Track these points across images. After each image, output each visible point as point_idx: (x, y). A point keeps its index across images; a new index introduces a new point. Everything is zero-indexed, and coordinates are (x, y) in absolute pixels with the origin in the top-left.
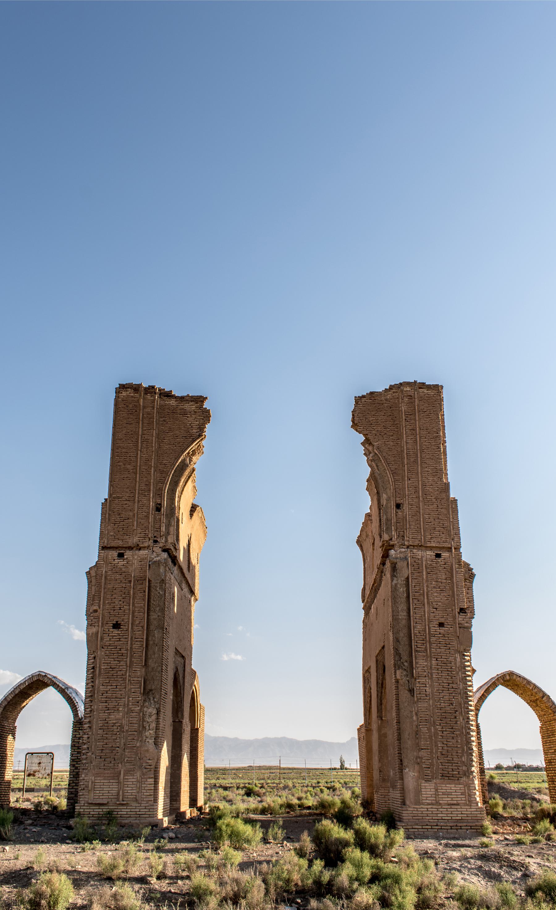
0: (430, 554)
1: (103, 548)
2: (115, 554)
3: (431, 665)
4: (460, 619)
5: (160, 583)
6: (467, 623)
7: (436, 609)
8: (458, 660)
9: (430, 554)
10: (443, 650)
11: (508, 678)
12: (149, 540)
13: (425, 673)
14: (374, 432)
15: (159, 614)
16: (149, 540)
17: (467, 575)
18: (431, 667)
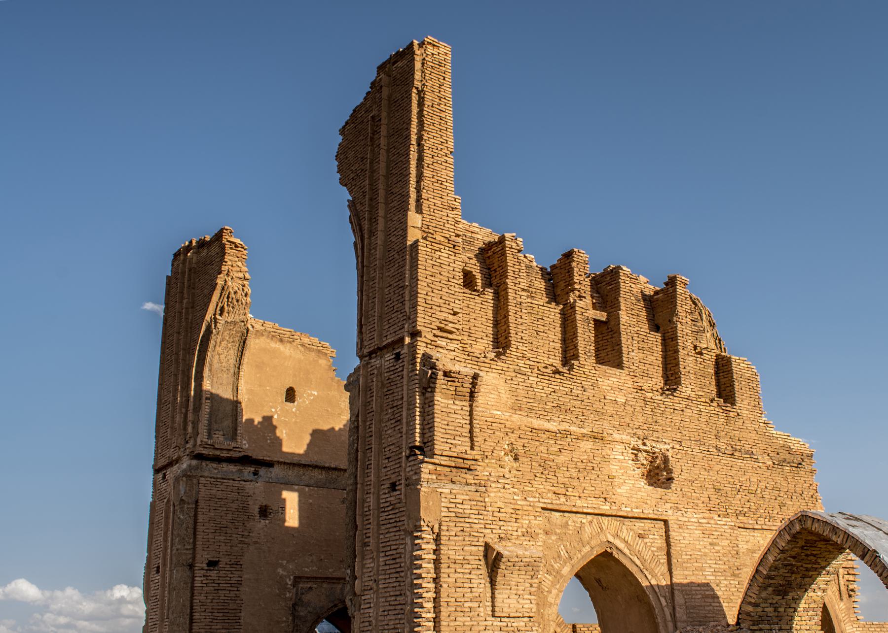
0: (389, 356)
1: (157, 471)
2: (160, 475)
3: (379, 566)
4: (408, 469)
6: (416, 473)
7: (388, 458)
8: (408, 548)
9: (389, 356)
10: (392, 534)
11: (798, 527)
13: (371, 583)
14: (352, 176)
17: (424, 380)
18: (378, 570)
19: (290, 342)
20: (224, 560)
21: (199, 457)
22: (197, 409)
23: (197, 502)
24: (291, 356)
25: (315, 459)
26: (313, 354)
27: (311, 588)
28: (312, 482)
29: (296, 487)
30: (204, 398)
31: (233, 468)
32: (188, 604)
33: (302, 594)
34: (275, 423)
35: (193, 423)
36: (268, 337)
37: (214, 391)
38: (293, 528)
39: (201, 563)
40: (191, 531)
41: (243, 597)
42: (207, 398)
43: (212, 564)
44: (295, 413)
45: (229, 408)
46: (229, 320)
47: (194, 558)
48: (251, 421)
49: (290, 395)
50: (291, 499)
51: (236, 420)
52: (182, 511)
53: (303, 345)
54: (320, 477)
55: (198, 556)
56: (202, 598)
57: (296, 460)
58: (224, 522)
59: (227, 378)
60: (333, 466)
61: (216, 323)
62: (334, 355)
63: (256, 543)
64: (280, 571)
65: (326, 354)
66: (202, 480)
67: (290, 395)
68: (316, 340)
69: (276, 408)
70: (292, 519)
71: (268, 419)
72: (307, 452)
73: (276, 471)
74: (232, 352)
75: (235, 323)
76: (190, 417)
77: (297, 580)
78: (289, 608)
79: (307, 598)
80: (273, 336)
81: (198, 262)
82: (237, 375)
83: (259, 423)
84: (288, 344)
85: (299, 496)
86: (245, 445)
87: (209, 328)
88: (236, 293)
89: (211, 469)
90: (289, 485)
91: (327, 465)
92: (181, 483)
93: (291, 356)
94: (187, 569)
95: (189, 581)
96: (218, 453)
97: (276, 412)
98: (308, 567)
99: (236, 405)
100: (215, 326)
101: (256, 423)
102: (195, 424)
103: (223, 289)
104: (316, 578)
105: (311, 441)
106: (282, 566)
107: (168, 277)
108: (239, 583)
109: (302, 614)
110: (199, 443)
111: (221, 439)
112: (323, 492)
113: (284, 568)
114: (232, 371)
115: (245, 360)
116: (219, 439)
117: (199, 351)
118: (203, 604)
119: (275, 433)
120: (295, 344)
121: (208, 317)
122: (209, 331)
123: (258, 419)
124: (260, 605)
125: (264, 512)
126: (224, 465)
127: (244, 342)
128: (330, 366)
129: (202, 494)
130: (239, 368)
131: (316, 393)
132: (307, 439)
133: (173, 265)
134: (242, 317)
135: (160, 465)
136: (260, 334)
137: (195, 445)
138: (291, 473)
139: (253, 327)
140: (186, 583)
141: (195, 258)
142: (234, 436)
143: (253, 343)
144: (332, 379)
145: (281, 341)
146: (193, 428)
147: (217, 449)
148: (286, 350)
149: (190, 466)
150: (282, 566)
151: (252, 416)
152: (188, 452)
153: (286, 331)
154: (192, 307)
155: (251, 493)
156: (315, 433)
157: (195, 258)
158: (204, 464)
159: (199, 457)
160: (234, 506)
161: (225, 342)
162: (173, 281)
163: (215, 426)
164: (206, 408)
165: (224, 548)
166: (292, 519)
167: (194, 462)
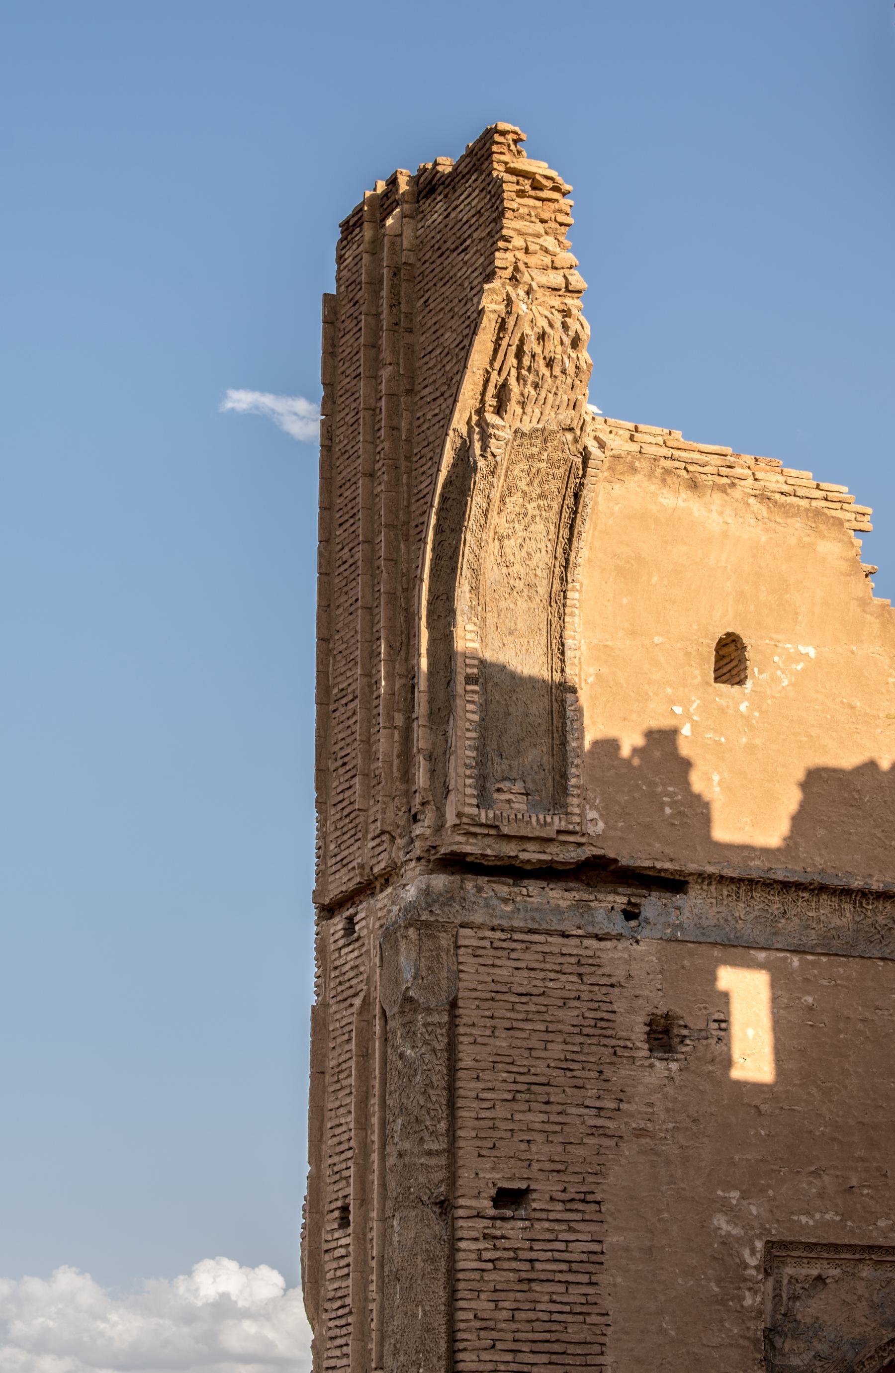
1: (327, 911)
2: (338, 924)
5: (402, 1012)
12: (393, 838)
15: (407, 1145)
16: (393, 838)
19: (723, 489)
20: (545, 1188)
21: (456, 864)
22: (442, 713)
23: (453, 1005)
24: (725, 535)
25: (815, 864)
26: (797, 523)
27: (820, 1278)
28: (812, 937)
29: (761, 956)
30: (461, 679)
31: (558, 896)
32: (439, 1323)
33: (795, 1298)
34: (685, 749)
35: (430, 758)
36: (651, 475)
37: (489, 655)
38: (758, 1088)
39: (475, 1199)
40: (439, 1096)
41: (608, 1304)
42: (469, 680)
43: (509, 1199)
44: (747, 719)
45: (538, 708)
46: (526, 427)
47: (452, 1179)
48: (609, 746)
49: (729, 660)
50: (748, 995)
51: (564, 744)
52: (410, 1034)
53: (763, 497)
54: (836, 921)
55: (465, 1176)
56: (483, 1305)
57: (756, 868)
58: (541, 1067)
59: (527, 612)
60: (876, 886)
61: (485, 438)
62: (866, 525)
63: (641, 1133)
64: (721, 1222)
65: (840, 522)
67: (729, 660)
68: (805, 478)
69: (686, 703)
70: (753, 1054)
71: (662, 740)
72: (791, 842)
73: (695, 904)
75: (545, 435)
76: (421, 738)
77: (777, 1251)
78: (755, 1342)
79: (809, 1309)
80: (667, 471)
81: (419, 246)
82: (558, 600)
83: (635, 751)
84: (717, 496)
85: (774, 985)
86: (595, 825)
88: (542, 337)
89: (490, 901)
90: (738, 949)
91: (857, 883)
92: (403, 945)
93: (725, 535)
94: (432, 1213)
95: (441, 1251)
96: (510, 849)
97: (688, 716)
98: (808, 1213)
100: (485, 447)
101: (626, 751)
102: (438, 760)
103: (502, 326)
104: (837, 1247)
105: (803, 806)
106: (726, 1207)
107: (326, 295)
108: (595, 1259)
109: (795, 1361)
110: (451, 819)
111: (520, 805)
112: (848, 970)
113: (734, 1214)
114: (543, 589)
115: (583, 552)
116: (513, 805)
117: (439, 530)
118: (486, 1325)
119: (687, 784)
120: (737, 493)
122: (464, 465)
123: (630, 742)
124: (661, 1331)
125: (663, 1035)
126: (533, 887)
127: (577, 496)
128: (854, 563)
129: (468, 980)
130: (564, 580)
131: (812, 652)
132: (791, 799)
133: (340, 259)
134: (566, 416)
135: (335, 890)
136: (623, 466)
137: (439, 828)
138: (744, 912)
139: (602, 445)
140: (431, 1259)
141: (408, 233)
142: (557, 795)
143: (604, 497)
144: (863, 603)
145: (694, 485)
146: (433, 772)
147: (509, 838)
148: (709, 513)
149: (427, 892)
150: (726, 1207)
151: (610, 732)
152: (418, 848)
153: (705, 452)
154: (410, 392)
155: (620, 974)
156: (817, 781)
157: (408, 233)
158: (469, 886)
159: (456, 864)
160: (568, 1016)
161: (517, 498)
162: (346, 309)
163: (499, 767)
164: (468, 710)
165: (541, 1150)
166: (753, 1054)
167: (440, 881)
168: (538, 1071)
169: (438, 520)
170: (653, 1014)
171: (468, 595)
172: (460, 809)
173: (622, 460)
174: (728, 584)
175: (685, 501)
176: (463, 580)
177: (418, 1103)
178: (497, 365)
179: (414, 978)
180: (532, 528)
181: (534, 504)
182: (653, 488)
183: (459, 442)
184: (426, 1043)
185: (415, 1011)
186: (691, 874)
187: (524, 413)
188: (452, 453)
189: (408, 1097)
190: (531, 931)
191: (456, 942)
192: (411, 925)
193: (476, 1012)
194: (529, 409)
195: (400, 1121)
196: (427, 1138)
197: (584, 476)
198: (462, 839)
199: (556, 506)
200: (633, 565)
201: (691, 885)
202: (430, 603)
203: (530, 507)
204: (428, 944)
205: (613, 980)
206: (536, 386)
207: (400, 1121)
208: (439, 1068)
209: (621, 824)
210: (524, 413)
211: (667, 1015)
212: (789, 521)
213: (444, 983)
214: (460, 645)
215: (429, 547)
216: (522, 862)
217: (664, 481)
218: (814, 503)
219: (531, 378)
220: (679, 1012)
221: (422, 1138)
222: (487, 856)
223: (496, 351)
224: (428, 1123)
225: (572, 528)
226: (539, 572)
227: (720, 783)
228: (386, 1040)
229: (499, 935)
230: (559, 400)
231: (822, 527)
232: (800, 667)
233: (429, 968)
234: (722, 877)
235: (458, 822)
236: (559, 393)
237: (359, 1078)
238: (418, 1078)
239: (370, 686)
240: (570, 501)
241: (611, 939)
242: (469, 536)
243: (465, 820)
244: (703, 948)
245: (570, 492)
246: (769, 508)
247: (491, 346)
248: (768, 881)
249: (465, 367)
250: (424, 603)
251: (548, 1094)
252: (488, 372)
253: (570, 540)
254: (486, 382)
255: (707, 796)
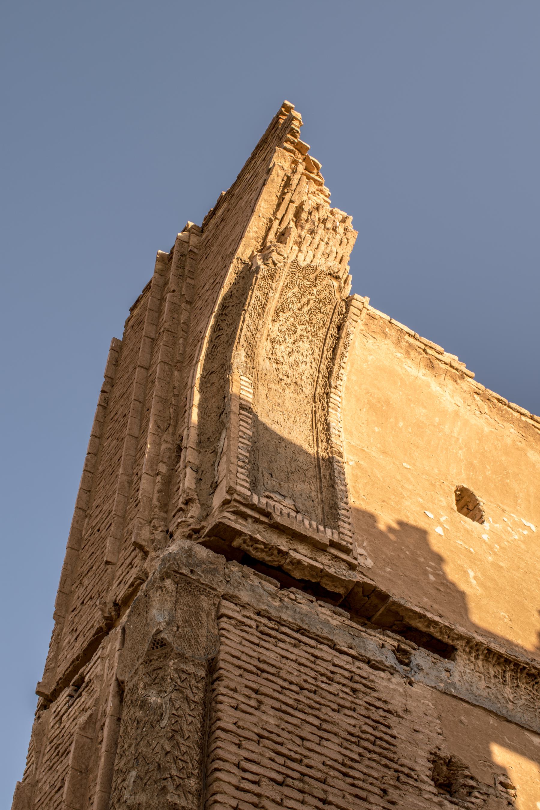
21: (222, 542)
36: (398, 343)
58: (316, 760)
66: (228, 608)
73: (463, 671)
74: (305, 346)
84: (449, 382)
87: (248, 274)
93: (457, 413)
99: (327, 471)
107: (115, 340)
114: (308, 390)
121: (246, 250)
122: (248, 274)
127: (339, 328)
130: (327, 385)
160: (345, 722)
168: (312, 763)
169: (217, 321)
170: (435, 754)
171: (243, 359)
172: (232, 484)
173: (376, 322)
174: (460, 452)
175: (424, 375)
176: (239, 347)
177: (163, 748)
178: (279, 216)
179: (168, 624)
180: (300, 344)
181: (303, 327)
182: (399, 355)
183: (241, 267)
184: (177, 689)
185: (166, 657)
186: (460, 637)
187: (300, 251)
188: (235, 276)
189: (149, 744)
190: (299, 630)
191: (218, 611)
192: (169, 577)
193: (239, 679)
194: (304, 248)
195: (134, 773)
196: (171, 788)
197: (347, 312)
198: (233, 517)
199: (321, 333)
200: (383, 406)
201: (458, 653)
202: (203, 377)
203: (300, 328)
204: (187, 599)
205: (390, 707)
206: (312, 232)
207: (134, 773)
208: (190, 719)
209: (388, 570)
210: (300, 251)
211: (450, 761)
212: (505, 424)
213: (203, 640)
214: (234, 390)
215: (206, 340)
216: (291, 562)
217: (408, 353)
218: (524, 418)
219: (308, 226)
220: (464, 761)
221: (164, 788)
222: (257, 541)
223: (279, 205)
224: (174, 772)
225: (334, 351)
226: (304, 378)
227: (475, 578)
228: (119, 719)
229: (265, 621)
230: (329, 248)
231: (530, 438)
232: (526, 532)
233: (187, 621)
234: (489, 650)
235: (228, 497)
236: (331, 243)
237: (73, 792)
238: (164, 723)
239: (130, 483)
240: (333, 331)
241: (384, 671)
242: (247, 316)
243: (236, 496)
244: (477, 711)
245: (334, 325)
246: (490, 407)
247: (275, 201)
248: (533, 671)
249: (253, 211)
250: (198, 376)
251: (325, 792)
252: (271, 221)
253: (333, 359)
254: (269, 229)
255: (462, 586)
